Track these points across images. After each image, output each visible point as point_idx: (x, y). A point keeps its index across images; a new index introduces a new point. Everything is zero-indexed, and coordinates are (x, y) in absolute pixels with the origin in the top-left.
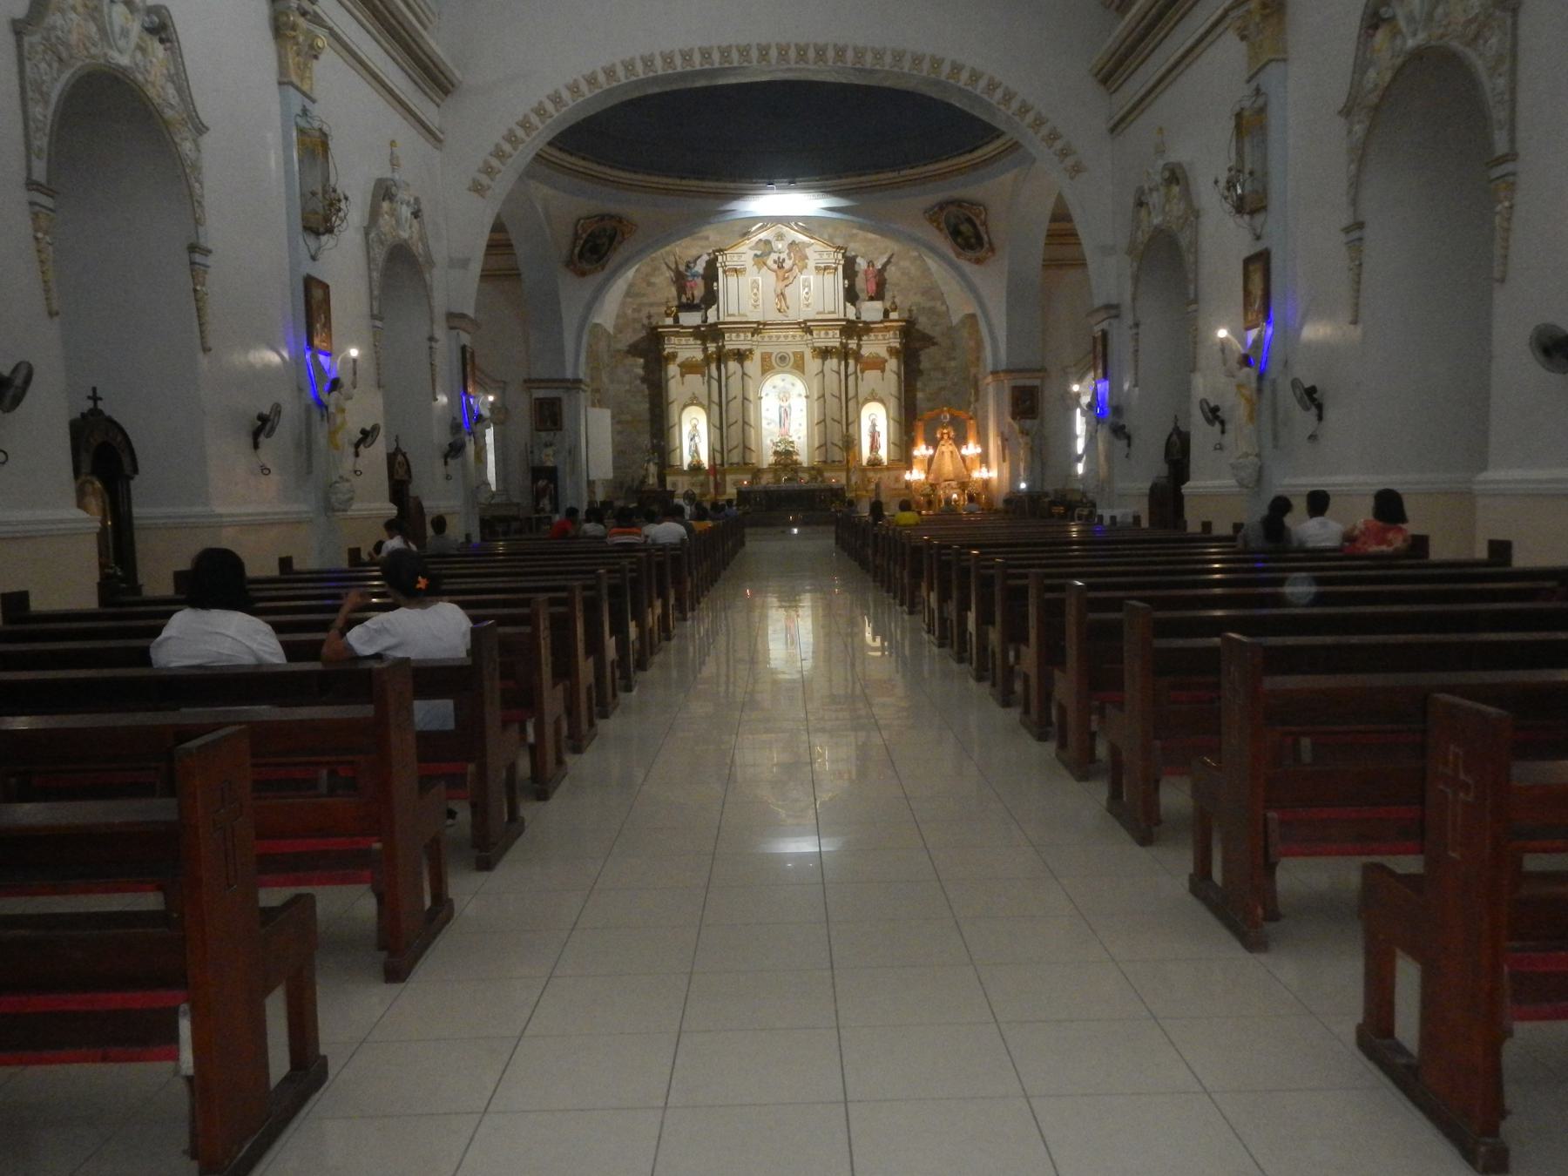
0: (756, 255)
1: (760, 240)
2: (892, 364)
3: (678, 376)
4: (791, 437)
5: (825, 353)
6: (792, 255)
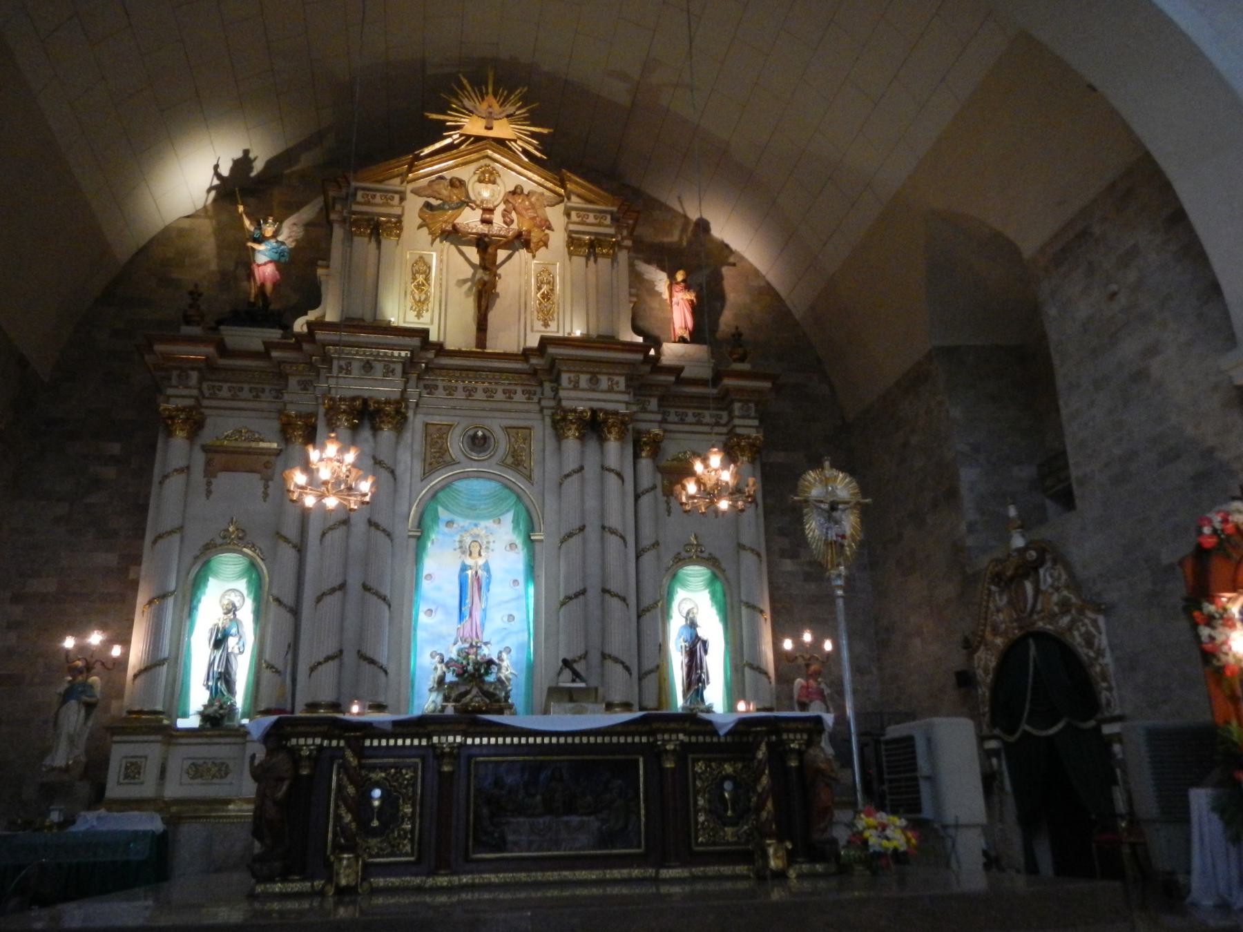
0: (428, 205)
1: (441, 178)
4: (486, 644)
6: (514, 215)
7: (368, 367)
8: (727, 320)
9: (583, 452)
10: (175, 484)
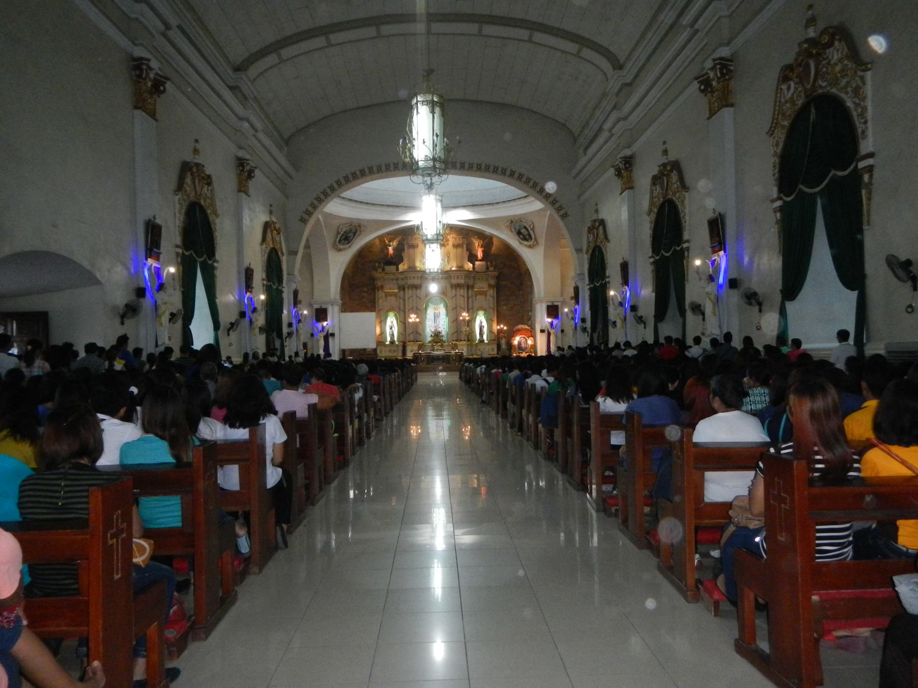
2: (492, 292)
3: (384, 298)
5: (458, 286)
7: (414, 278)
8: (493, 248)
9: (456, 292)
10: (380, 301)
